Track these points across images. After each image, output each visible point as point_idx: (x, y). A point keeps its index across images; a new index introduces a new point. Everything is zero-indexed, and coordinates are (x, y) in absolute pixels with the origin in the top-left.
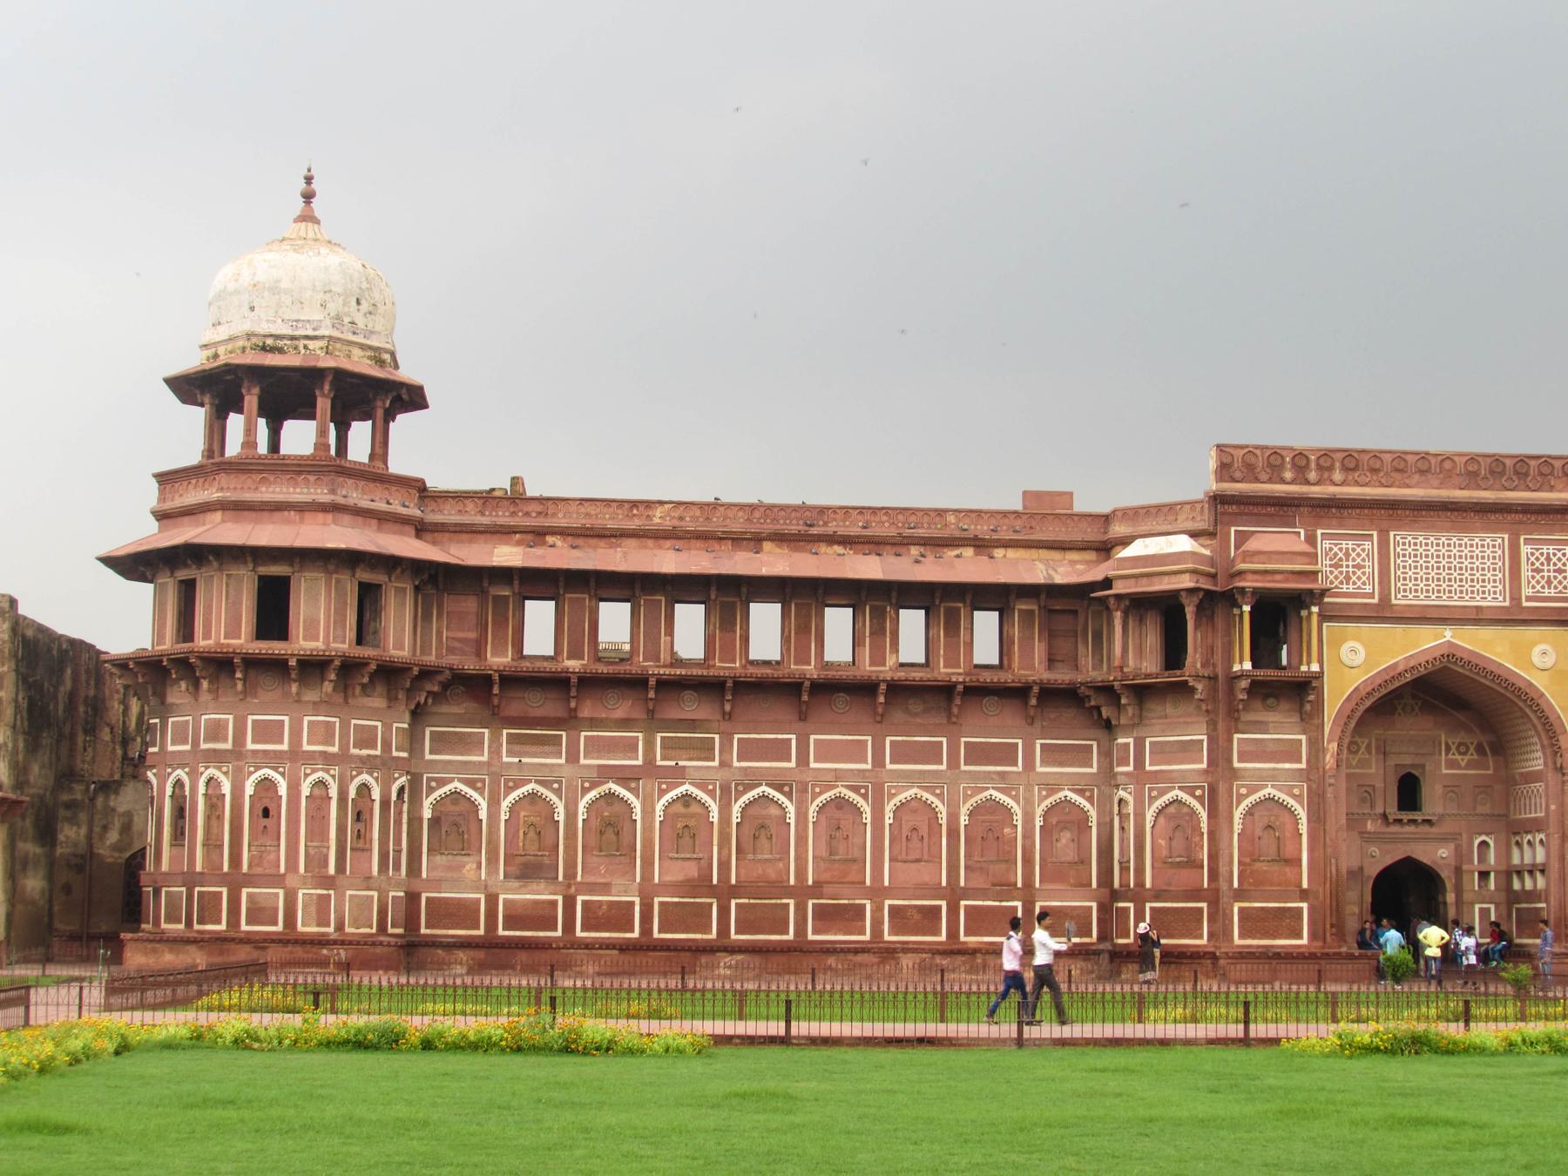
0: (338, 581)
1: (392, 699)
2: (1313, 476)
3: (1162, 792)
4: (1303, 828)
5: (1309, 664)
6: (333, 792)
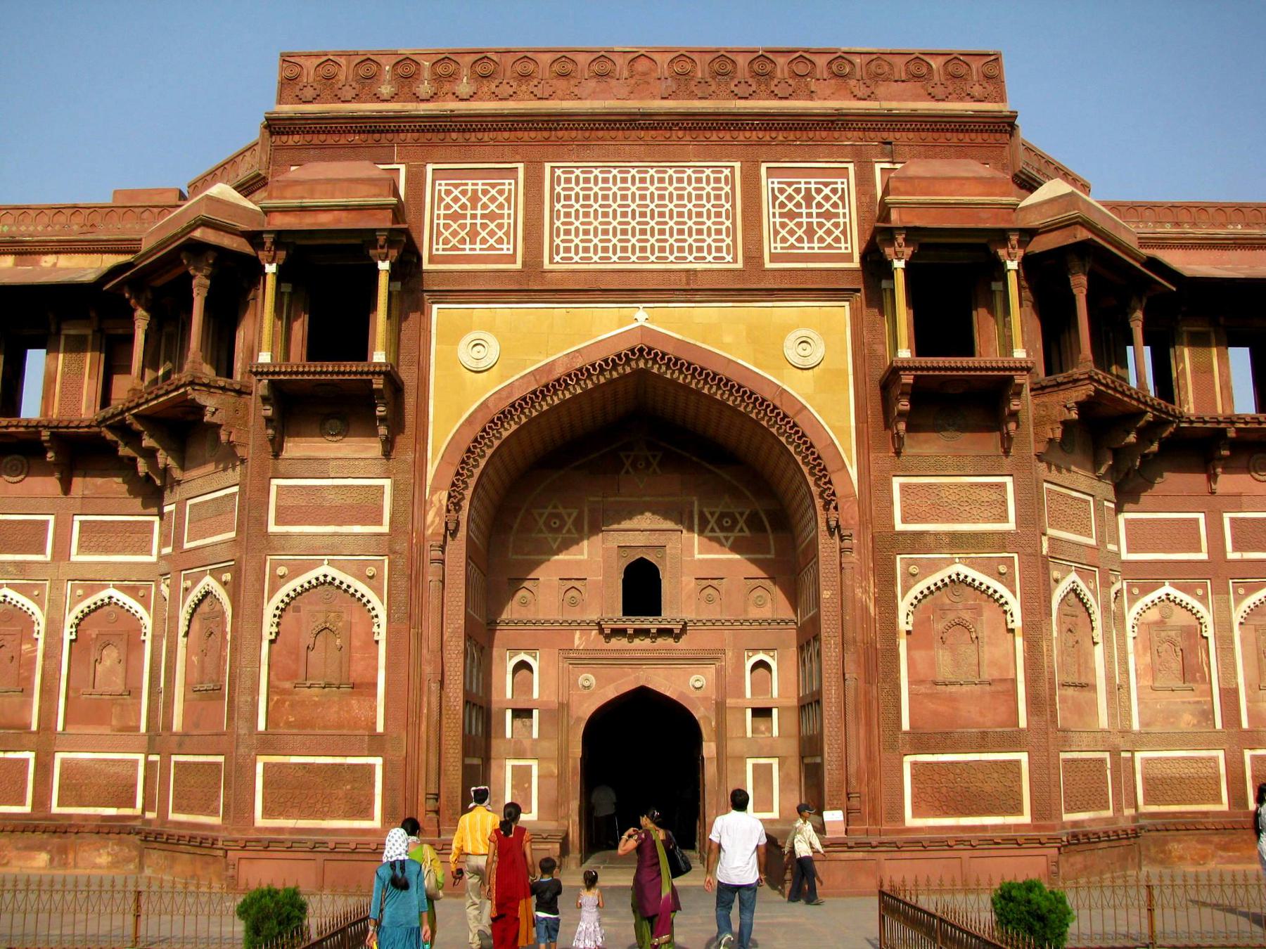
2: (425, 88)
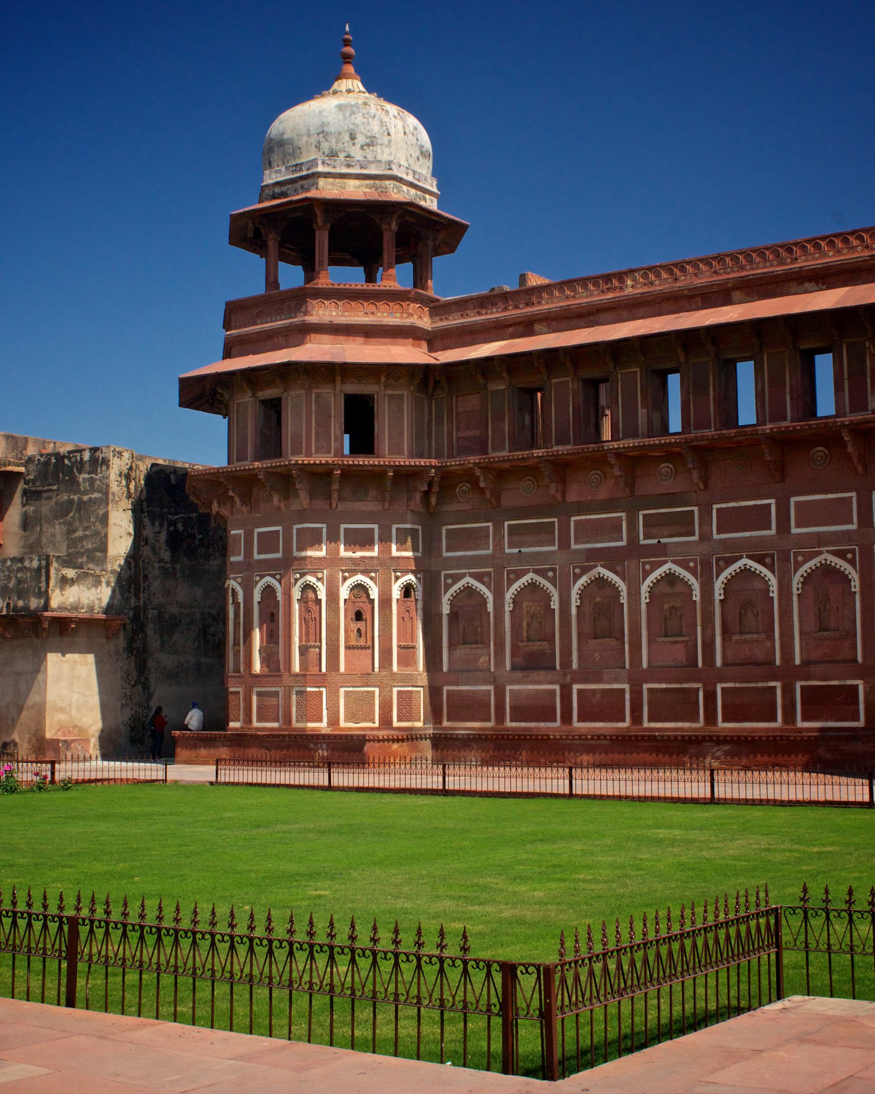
0: (318, 396)
6: (322, 595)
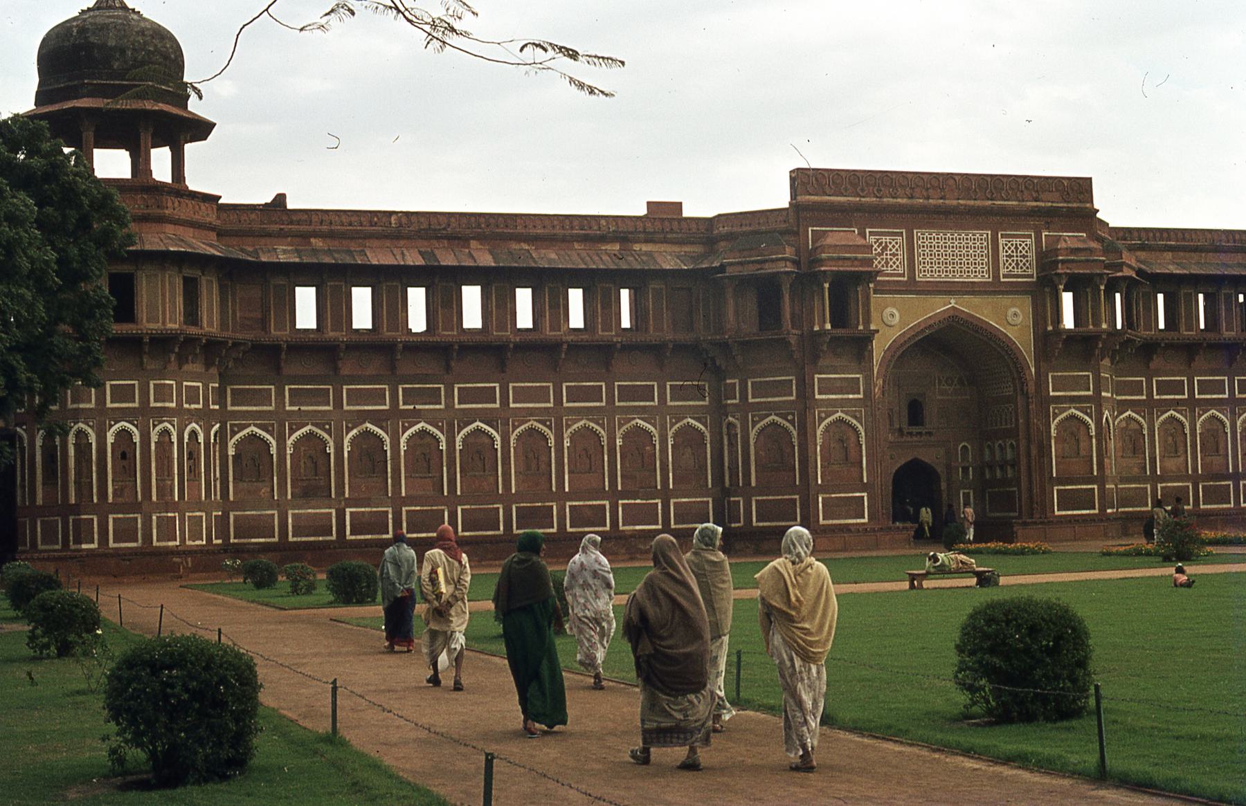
1: (208, 365)
3: (763, 418)
4: (863, 441)
5: (867, 321)
6: (174, 439)
